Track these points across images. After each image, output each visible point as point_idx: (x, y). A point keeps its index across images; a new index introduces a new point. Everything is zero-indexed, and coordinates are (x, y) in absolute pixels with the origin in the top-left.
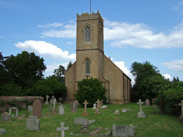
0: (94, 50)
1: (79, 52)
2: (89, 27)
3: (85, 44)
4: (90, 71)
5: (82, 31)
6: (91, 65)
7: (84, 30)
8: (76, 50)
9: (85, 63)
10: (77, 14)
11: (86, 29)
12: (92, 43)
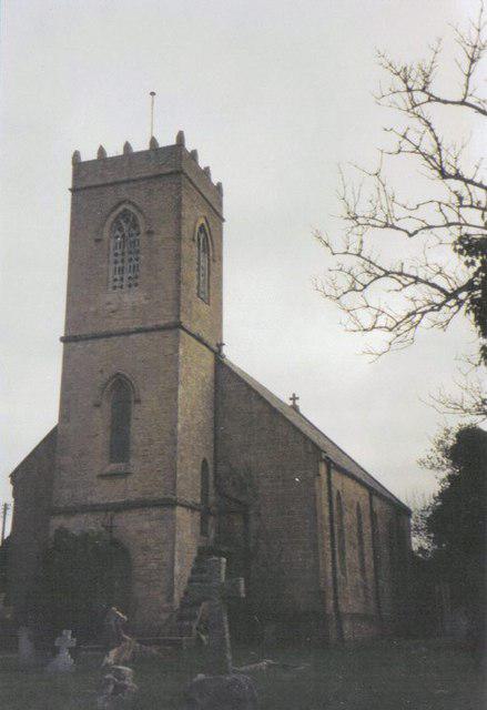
0: (157, 336)
1: (80, 345)
2: (135, 219)
3: (109, 303)
4: (133, 447)
5: (98, 241)
6: (136, 410)
7: (106, 235)
8: (63, 340)
9: (106, 405)
10: (76, 155)
11: (120, 229)
12: (146, 299)
